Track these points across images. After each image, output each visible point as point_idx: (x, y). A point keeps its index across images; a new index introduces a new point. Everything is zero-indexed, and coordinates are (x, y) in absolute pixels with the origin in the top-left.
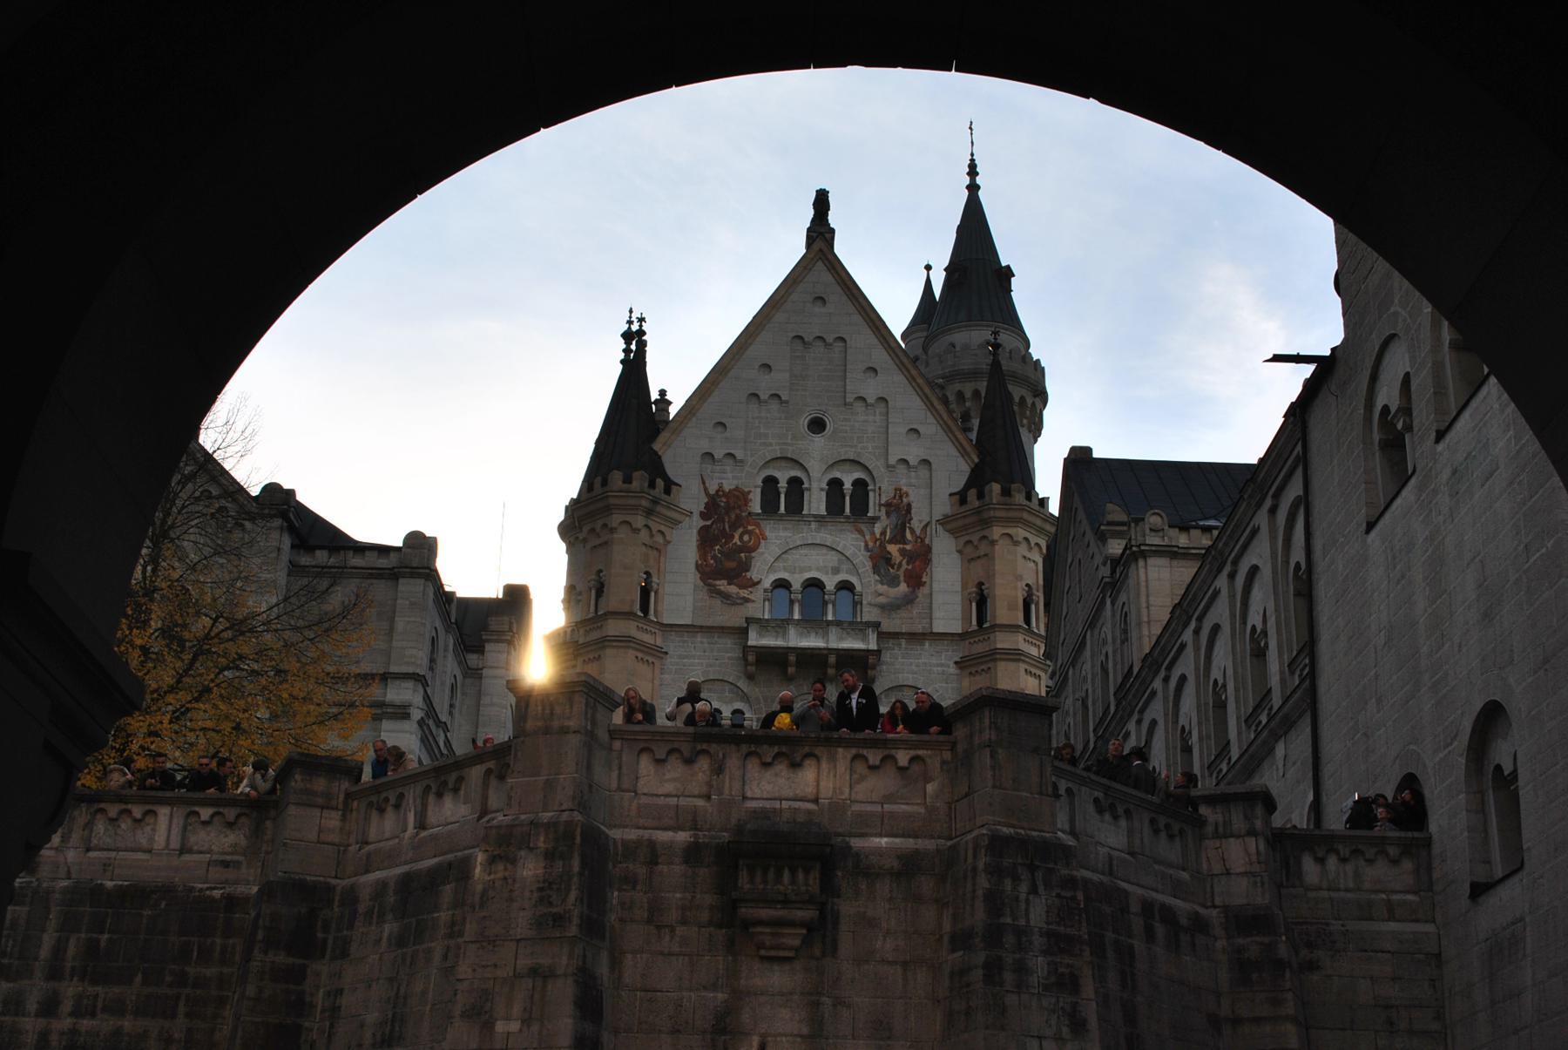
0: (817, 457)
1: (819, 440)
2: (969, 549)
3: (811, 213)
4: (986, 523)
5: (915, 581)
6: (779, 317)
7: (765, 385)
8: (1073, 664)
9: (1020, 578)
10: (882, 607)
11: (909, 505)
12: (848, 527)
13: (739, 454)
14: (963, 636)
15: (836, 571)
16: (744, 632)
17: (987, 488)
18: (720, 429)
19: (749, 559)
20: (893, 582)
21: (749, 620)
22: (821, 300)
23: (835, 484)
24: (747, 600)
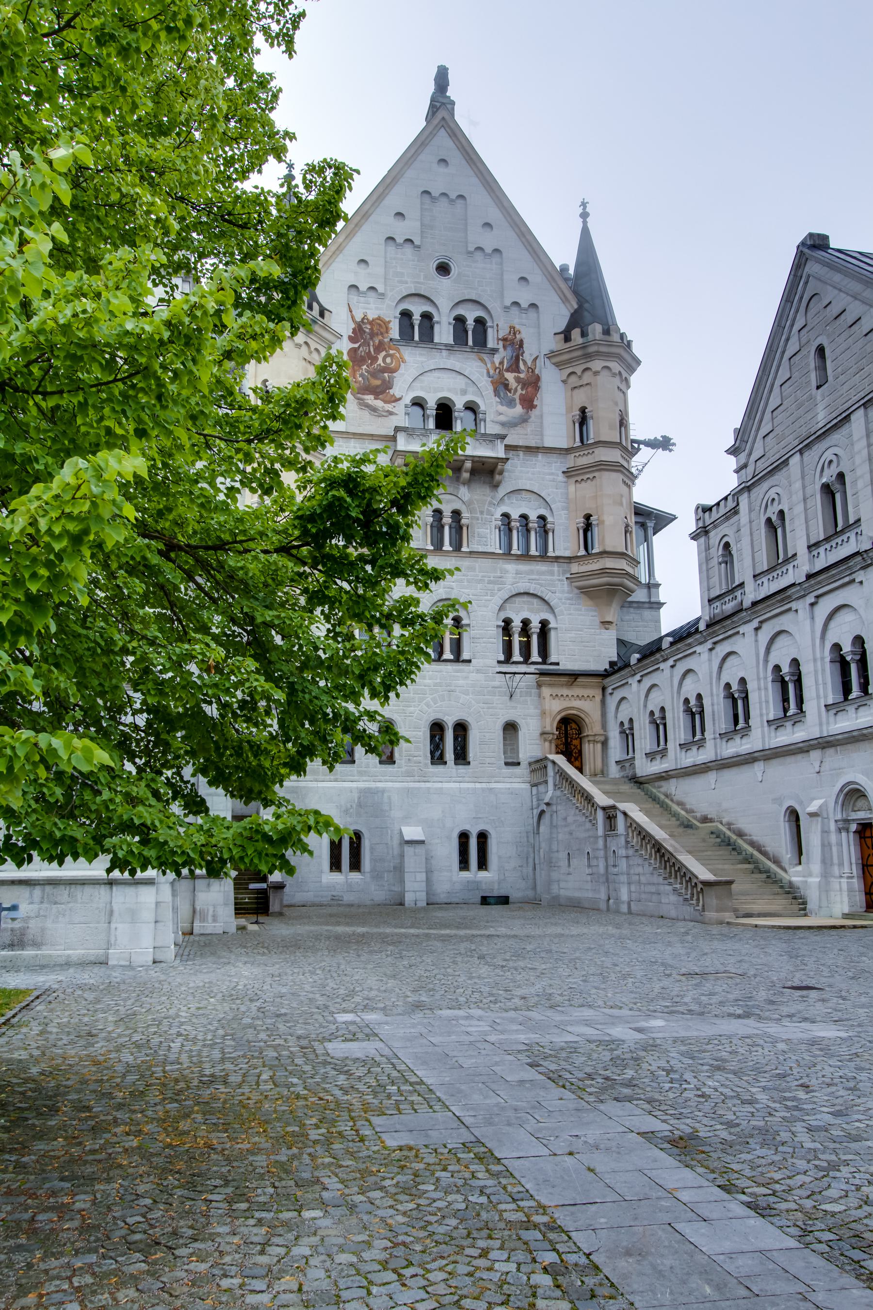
0: (445, 297)
1: (445, 282)
2: (573, 380)
3: (431, 88)
4: (588, 357)
5: (529, 403)
6: (410, 174)
7: (401, 230)
8: (801, 452)
9: (616, 404)
10: (503, 424)
11: (521, 341)
12: (473, 356)
13: (381, 289)
14: (568, 451)
15: (464, 392)
16: (394, 439)
17: (590, 328)
18: (363, 265)
19: (391, 379)
20: (511, 403)
21: (397, 429)
22: (443, 161)
23: (460, 320)
24: (391, 413)
